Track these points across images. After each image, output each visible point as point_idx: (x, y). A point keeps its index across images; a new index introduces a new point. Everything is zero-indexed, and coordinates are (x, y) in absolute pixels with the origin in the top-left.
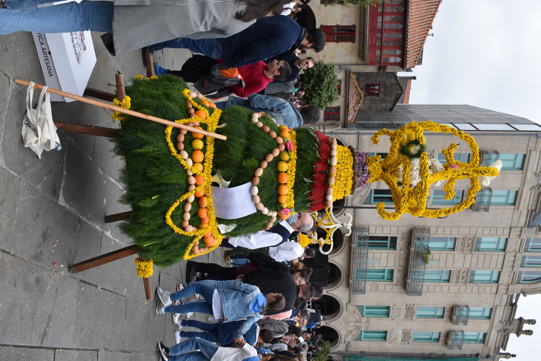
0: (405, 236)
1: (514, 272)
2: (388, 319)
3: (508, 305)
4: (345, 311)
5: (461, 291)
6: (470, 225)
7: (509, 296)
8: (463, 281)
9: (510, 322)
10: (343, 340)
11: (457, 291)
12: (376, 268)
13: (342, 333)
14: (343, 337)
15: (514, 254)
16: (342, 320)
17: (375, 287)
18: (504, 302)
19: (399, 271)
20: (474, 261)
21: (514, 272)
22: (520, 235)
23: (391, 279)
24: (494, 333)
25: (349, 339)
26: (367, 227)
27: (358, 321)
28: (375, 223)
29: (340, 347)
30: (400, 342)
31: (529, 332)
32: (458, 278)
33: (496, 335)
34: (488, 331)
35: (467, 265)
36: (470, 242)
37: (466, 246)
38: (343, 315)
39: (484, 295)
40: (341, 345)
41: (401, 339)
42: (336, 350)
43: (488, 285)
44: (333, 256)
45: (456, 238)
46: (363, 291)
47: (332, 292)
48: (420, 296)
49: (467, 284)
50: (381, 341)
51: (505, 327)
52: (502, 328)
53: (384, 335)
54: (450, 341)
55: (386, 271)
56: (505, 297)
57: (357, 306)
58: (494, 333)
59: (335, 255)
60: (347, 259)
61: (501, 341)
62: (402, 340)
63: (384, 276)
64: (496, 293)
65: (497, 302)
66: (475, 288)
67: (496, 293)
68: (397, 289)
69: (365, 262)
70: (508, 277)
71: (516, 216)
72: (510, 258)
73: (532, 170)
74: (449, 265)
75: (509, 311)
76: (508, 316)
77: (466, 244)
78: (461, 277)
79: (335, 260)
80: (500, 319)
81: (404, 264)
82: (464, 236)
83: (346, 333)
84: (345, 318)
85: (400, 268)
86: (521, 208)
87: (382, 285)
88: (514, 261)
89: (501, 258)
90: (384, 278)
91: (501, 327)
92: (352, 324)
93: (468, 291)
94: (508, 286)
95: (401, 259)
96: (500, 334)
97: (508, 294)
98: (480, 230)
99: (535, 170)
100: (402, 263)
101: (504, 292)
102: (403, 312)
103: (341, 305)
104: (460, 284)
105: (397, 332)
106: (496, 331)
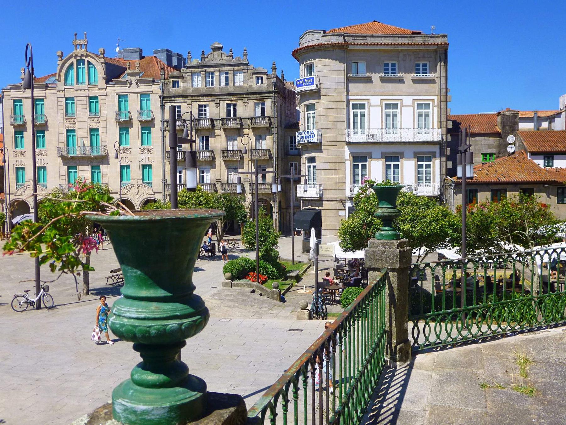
10: (152, 196)
14: (149, 196)
17: (105, 177)
20: (82, 115)
22: (62, 91)
25: (151, 192)
37: (71, 123)
58: (138, 90)
67: (106, 96)
71: (51, 96)
73: (22, 94)
74: (86, 131)
86: (44, 95)
88: (81, 90)
94: (99, 89)
98: (60, 116)
99: (22, 92)
101: (104, 91)
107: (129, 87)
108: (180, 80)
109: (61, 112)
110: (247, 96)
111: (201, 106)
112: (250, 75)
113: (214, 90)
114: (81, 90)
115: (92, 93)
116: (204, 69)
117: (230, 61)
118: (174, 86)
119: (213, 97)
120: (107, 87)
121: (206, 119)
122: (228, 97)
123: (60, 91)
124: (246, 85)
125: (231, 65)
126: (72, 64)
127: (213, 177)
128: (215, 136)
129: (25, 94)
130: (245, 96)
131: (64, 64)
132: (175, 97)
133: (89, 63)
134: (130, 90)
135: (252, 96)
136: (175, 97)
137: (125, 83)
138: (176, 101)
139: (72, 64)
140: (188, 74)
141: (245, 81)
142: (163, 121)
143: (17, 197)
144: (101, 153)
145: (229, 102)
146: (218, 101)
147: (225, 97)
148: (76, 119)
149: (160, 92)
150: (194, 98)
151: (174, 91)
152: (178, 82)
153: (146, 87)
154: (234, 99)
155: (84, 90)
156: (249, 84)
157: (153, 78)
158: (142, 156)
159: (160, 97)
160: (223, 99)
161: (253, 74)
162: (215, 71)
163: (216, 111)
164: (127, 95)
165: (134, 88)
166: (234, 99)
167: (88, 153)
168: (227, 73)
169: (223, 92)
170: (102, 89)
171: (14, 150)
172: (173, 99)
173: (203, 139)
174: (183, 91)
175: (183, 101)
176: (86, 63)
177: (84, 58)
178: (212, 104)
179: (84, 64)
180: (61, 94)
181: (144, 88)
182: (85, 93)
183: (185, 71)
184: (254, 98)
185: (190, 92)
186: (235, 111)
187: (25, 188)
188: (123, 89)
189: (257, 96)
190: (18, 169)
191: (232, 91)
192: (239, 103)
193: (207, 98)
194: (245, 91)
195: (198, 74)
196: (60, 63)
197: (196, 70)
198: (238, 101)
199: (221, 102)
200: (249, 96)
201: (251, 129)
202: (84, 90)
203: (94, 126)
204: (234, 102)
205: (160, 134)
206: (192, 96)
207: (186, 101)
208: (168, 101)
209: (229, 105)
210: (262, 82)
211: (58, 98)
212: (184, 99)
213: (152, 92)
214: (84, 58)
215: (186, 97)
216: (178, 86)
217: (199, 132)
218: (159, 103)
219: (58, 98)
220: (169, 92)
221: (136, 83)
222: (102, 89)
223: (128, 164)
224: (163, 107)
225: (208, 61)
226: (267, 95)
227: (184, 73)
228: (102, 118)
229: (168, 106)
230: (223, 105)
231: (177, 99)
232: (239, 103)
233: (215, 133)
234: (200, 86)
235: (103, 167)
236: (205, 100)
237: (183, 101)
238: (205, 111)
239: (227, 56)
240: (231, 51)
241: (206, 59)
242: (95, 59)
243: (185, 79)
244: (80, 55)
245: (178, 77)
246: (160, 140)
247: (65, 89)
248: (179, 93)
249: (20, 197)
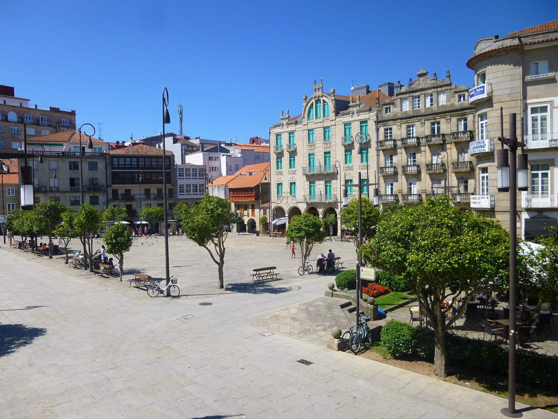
20: (319, 142)
22: (306, 125)
35: (321, 145)
58: (359, 118)
67: (335, 125)
73: (280, 130)
88: (318, 123)
94: (331, 121)
101: (334, 122)
107: (352, 117)
108: (391, 106)
109: (305, 141)
110: (450, 114)
111: (408, 127)
112: (453, 94)
113: (420, 112)
114: (318, 123)
115: (326, 124)
116: (411, 94)
117: (434, 83)
118: (387, 112)
119: (419, 118)
120: (336, 118)
121: (413, 138)
122: (432, 116)
123: (304, 125)
124: (449, 104)
125: (435, 88)
126: (312, 105)
127: (419, 188)
128: (420, 152)
129: (284, 129)
130: (447, 114)
131: (307, 104)
132: (387, 121)
133: (324, 101)
134: (352, 119)
135: (455, 113)
136: (387, 121)
137: (349, 113)
138: (388, 124)
139: (312, 105)
140: (398, 100)
141: (448, 100)
142: (378, 142)
143: (278, 205)
144: (331, 171)
145: (433, 121)
146: (424, 121)
147: (430, 117)
148: (315, 145)
149: (375, 117)
150: (402, 120)
151: (386, 116)
152: (390, 108)
153: (364, 115)
154: (438, 117)
155: (321, 122)
156: (452, 102)
157: (370, 108)
159: (375, 122)
160: (427, 119)
161: (456, 92)
162: (420, 95)
163: (421, 129)
164: (350, 123)
165: (356, 117)
166: (438, 117)
167: (323, 171)
168: (431, 95)
169: (428, 112)
170: (333, 120)
171: (277, 171)
172: (385, 123)
173: (411, 155)
174: (394, 115)
175: (393, 124)
176: (322, 101)
177: (320, 98)
178: (418, 124)
179: (320, 103)
180: (305, 127)
181: (363, 116)
182: (321, 125)
183: (395, 98)
184: (456, 115)
185: (399, 115)
186: (439, 128)
187: (283, 198)
188: (347, 119)
189: (460, 112)
190: (278, 184)
191: (435, 111)
192: (443, 121)
193: (413, 119)
194: (448, 109)
195: (406, 99)
196: (305, 104)
197: (405, 96)
198: (442, 119)
199: (426, 122)
200: (452, 113)
201: (453, 144)
202: (321, 122)
203: (327, 150)
204: (437, 120)
205: (375, 152)
206: (401, 119)
207: (396, 123)
208: (382, 125)
209: (433, 124)
210: (464, 99)
211: (303, 130)
212: (394, 122)
213: (369, 118)
214: (320, 98)
215: (396, 120)
216: (390, 112)
217: (407, 150)
218: (374, 127)
219: (303, 130)
220: (382, 117)
221: (357, 113)
222: (333, 120)
223: (351, 179)
224: (378, 130)
225: (415, 86)
226: (468, 111)
227: (394, 100)
228: (333, 143)
229: (382, 130)
230: (428, 124)
231: (389, 122)
232: (443, 121)
233: (421, 149)
234: (408, 109)
235: (334, 182)
236: (412, 121)
237: (393, 124)
238: (413, 130)
239: (431, 80)
240: (435, 74)
241: (413, 85)
242: (328, 98)
243: (395, 105)
244: (317, 96)
245: (389, 104)
246: (375, 158)
247: (308, 123)
248: (391, 117)
249: (279, 205)
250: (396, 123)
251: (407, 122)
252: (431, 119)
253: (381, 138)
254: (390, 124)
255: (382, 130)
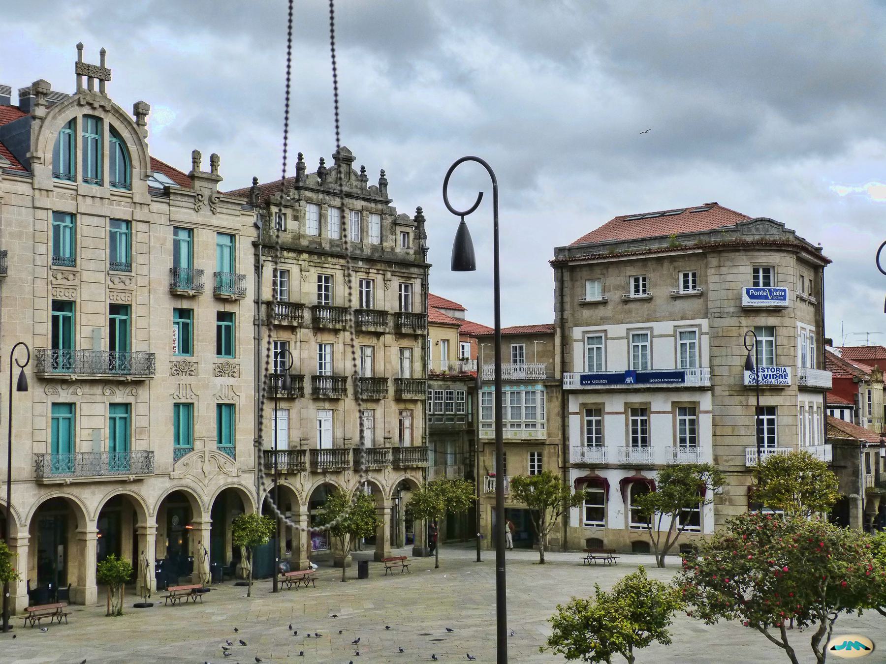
0: (50, 390)
1: (112, 195)
2: (196, 405)
3: (168, 201)
4: (183, 482)
5: (146, 284)
6: (30, 278)
7: (152, 201)
8: (127, 281)
9: (198, 195)
10: (236, 480)
11: (146, 290)
12: (107, 435)
13: (222, 482)
14: (230, 480)
15: (80, 198)
16: (201, 484)
18: (164, 208)
19: (113, 394)
20: (92, 265)
21: (112, 195)
22: (47, 191)
23: (127, 406)
24: (216, 221)
25: (233, 471)
26: (35, 458)
27: (202, 457)
28: (28, 443)
29: (248, 483)
30: (235, 379)
31: (214, 160)
32: (123, 291)
33: (221, 216)
34: (214, 231)
35: (101, 277)
36: (59, 276)
38: (192, 485)
39: (152, 244)
40: (243, 482)
41: (231, 379)
42: (253, 489)
43: (134, 237)
44: (88, 512)
45: (55, 303)
46: (148, 455)
47: (152, 507)
48: (156, 355)
49: (133, 274)
50: (235, 412)
51: (206, 202)
52: (209, 208)
53: (226, 410)
54: (232, 296)
55: (114, 416)
56: (155, 206)
57: (176, 460)
58: (216, 221)
59: (86, 509)
60: (93, 488)
61: (230, 206)
62: (232, 376)
63: (120, 418)
64: (148, 222)
65: (164, 220)
66: (140, 259)
68: (143, 392)
69: (98, 456)
70: (119, 205)
71: (14, 200)
72: (85, 206)
75: (178, 198)
76: (187, 199)
77: (65, 282)
78: (121, 286)
79: (94, 511)
80: (192, 211)
81: (100, 387)
82: (50, 287)
83: (222, 476)
84: (197, 481)
85: (108, 392)
87: (137, 421)
89: (87, 220)
90: (125, 418)
91: (206, 210)
92: (207, 468)
93: (145, 272)
94: (135, 203)
95: (92, 392)
96: (218, 210)
97: (149, 202)
100: (98, 390)
102: (185, 379)
103: (174, 490)
104: (132, 286)
105: (219, 387)
106: (214, 216)
108: (289, 212)
109: (42, 249)
115: (122, 211)
158: (219, 381)
159: (255, 245)
207: (300, 262)
224: (258, 268)
229: (268, 270)
237: (295, 261)
250: (300, 262)
251: (321, 265)
252: (362, 270)
253: (267, 295)
254: (287, 261)
255: (268, 270)
